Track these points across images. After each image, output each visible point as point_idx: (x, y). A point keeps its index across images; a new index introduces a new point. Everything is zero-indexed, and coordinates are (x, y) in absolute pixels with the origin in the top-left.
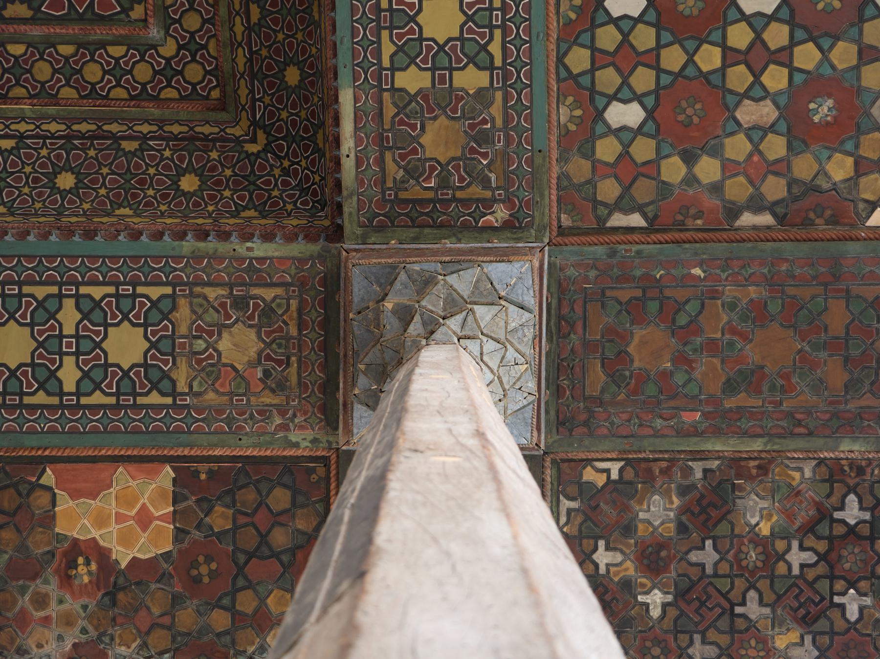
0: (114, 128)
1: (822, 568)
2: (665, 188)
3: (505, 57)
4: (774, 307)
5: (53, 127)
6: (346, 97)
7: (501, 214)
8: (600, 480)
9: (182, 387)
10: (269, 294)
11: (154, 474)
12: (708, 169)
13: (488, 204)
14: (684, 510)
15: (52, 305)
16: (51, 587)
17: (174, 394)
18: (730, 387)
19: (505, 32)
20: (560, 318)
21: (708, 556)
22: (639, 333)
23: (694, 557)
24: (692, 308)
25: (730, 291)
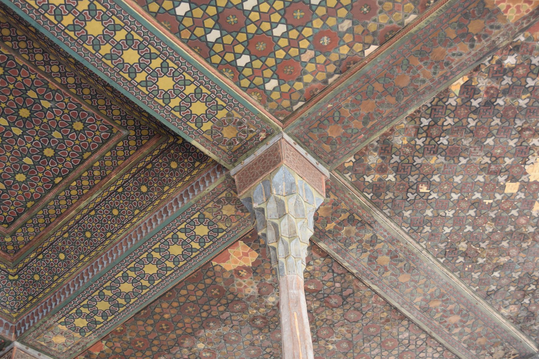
0: (141, 165)
1: (428, 139)
2: (301, 91)
3: (225, 103)
4: (359, 97)
5: (127, 177)
6: (194, 143)
7: (263, 135)
8: (351, 164)
9: (224, 228)
10: (224, 195)
11: (238, 245)
12: (308, 78)
13: (258, 135)
14: (380, 154)
15: (175, 236)
16: (240, 280)
17: (224, 231)
18: (365, 123)
19: (219, 97)
20: (304, 143)
21: (396, 158)
22: (328, 131)
23: (392, 161)
24: (337, 114)
25: (343, 104)
